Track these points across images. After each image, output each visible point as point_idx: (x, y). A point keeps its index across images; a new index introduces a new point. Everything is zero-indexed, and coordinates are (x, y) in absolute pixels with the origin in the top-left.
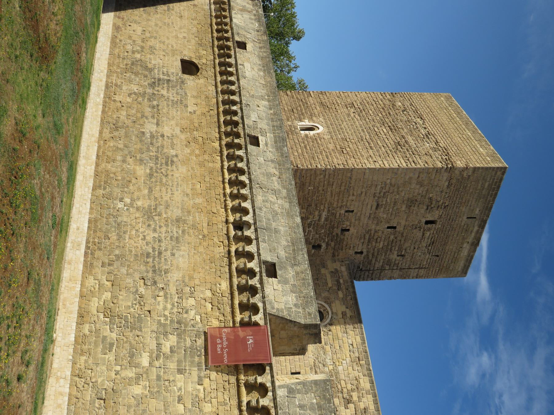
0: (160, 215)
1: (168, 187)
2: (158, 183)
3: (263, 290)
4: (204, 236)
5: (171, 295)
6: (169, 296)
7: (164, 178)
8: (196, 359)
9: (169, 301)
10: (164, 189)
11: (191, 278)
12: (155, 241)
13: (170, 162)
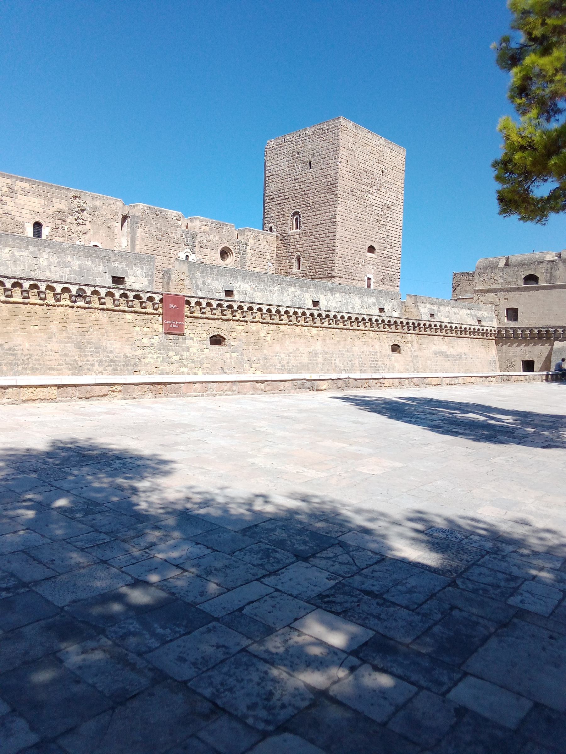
0: (76, 361)
1: (44, 354)
2: (42, 363)
3: (137, 291)
4: (90, 327)
5: (143, 354)
6: (143, 356)
7: (33, 358)
8: (181, 340)
9: (146, 355)
10: (47, 358)
11: (128, 340)
12: (102, 365)
13: (11, 352)
